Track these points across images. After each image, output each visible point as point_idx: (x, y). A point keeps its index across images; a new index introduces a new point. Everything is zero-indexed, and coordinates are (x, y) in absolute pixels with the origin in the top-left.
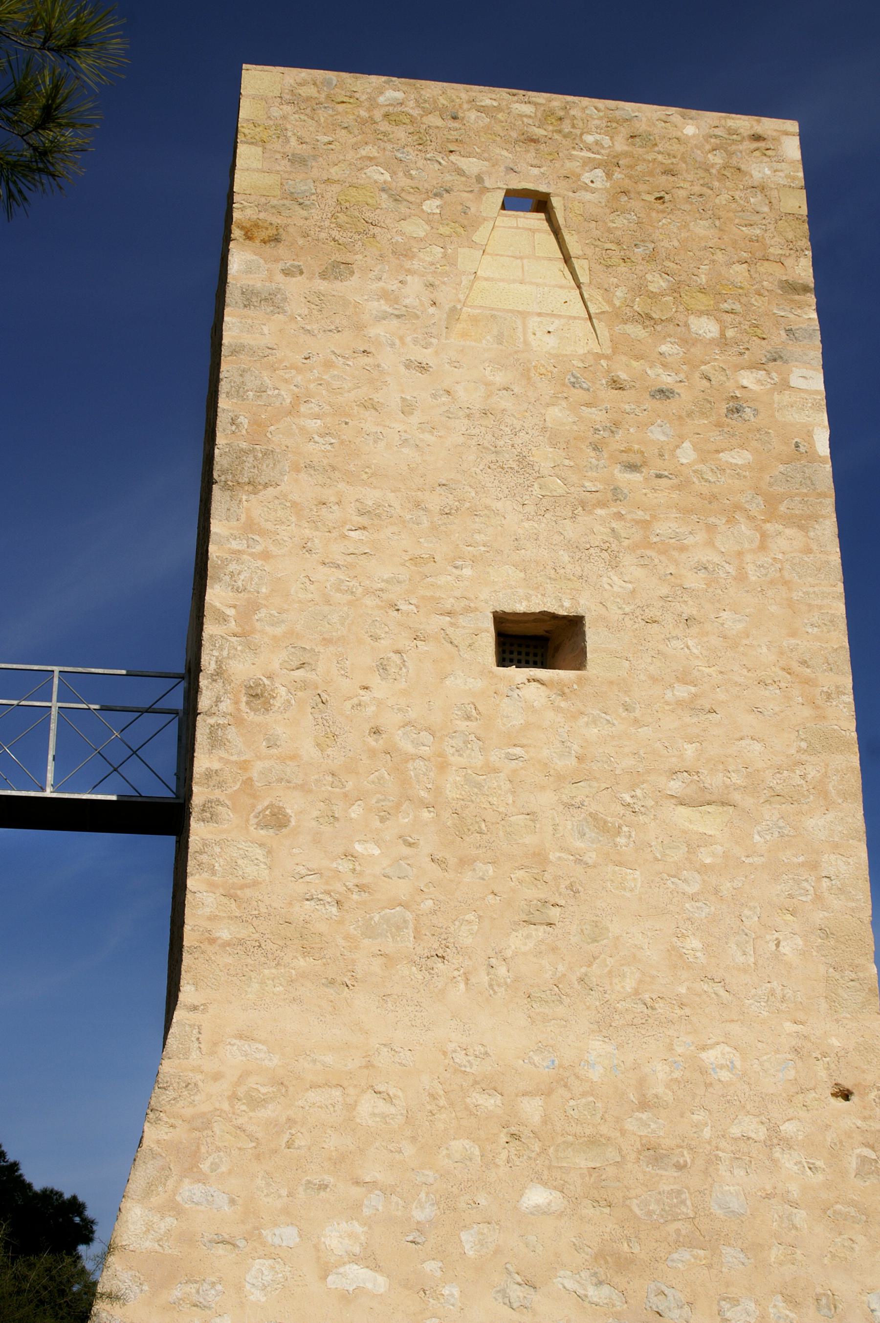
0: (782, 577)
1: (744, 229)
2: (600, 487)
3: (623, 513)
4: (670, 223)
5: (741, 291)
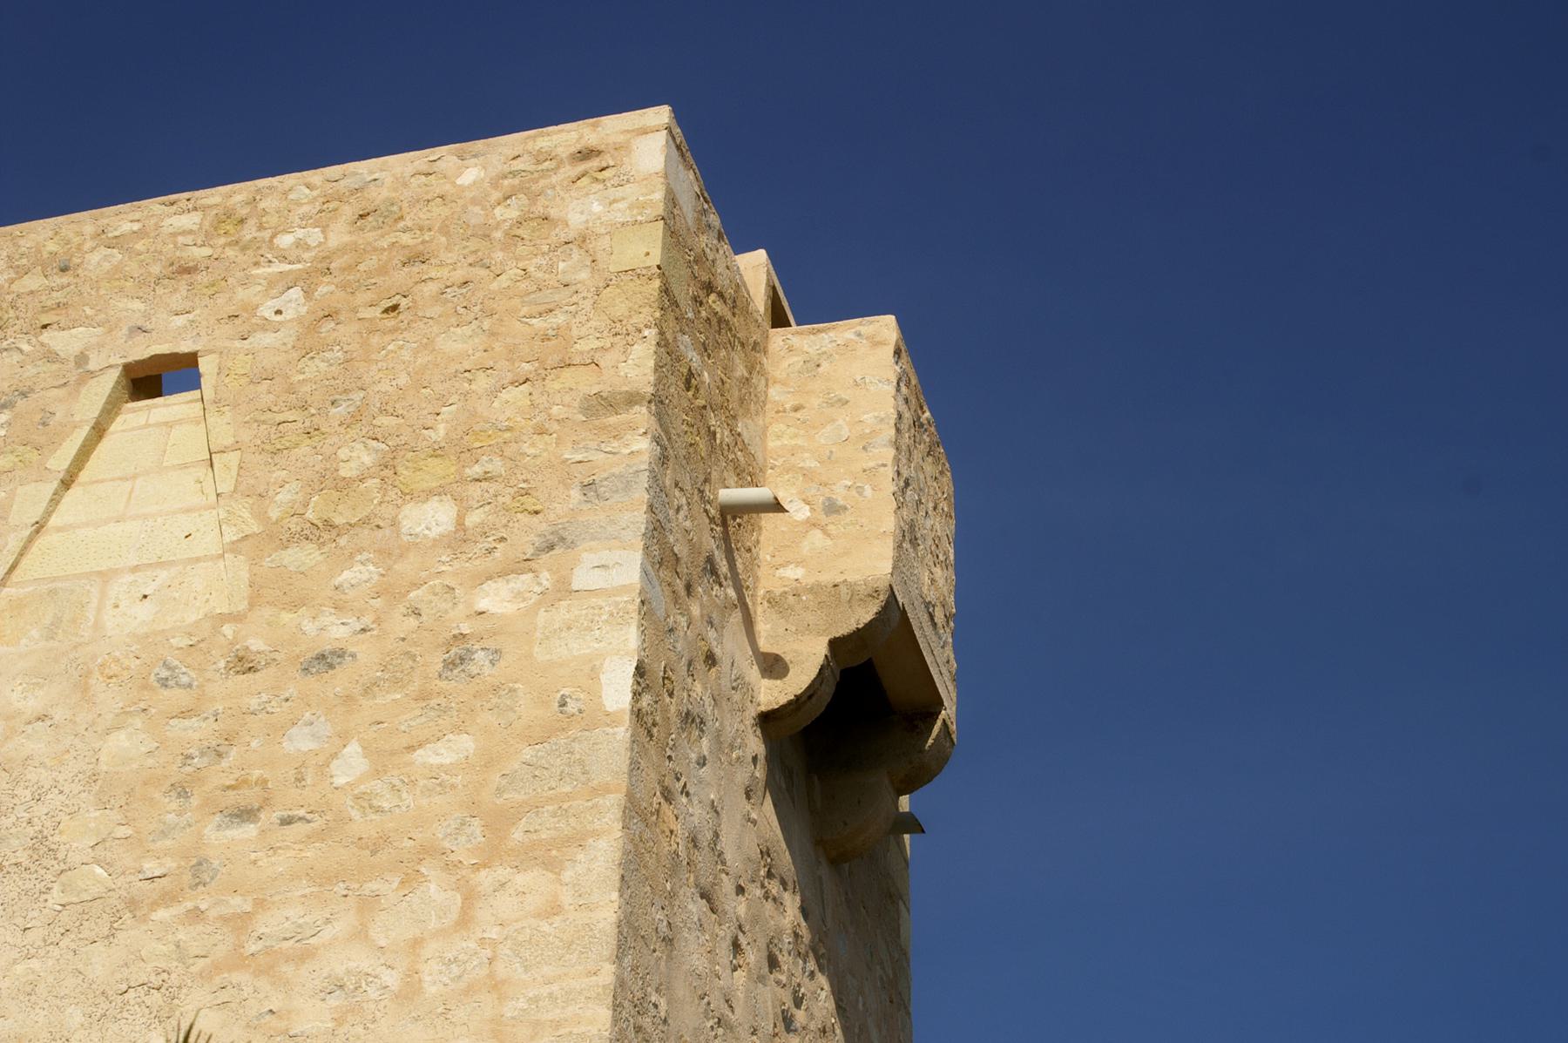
0: (491, 975)
1: (534, 321)
2: (170, 864)
3: (203, 907)
4: (401, 348)
5: (507, 435)
